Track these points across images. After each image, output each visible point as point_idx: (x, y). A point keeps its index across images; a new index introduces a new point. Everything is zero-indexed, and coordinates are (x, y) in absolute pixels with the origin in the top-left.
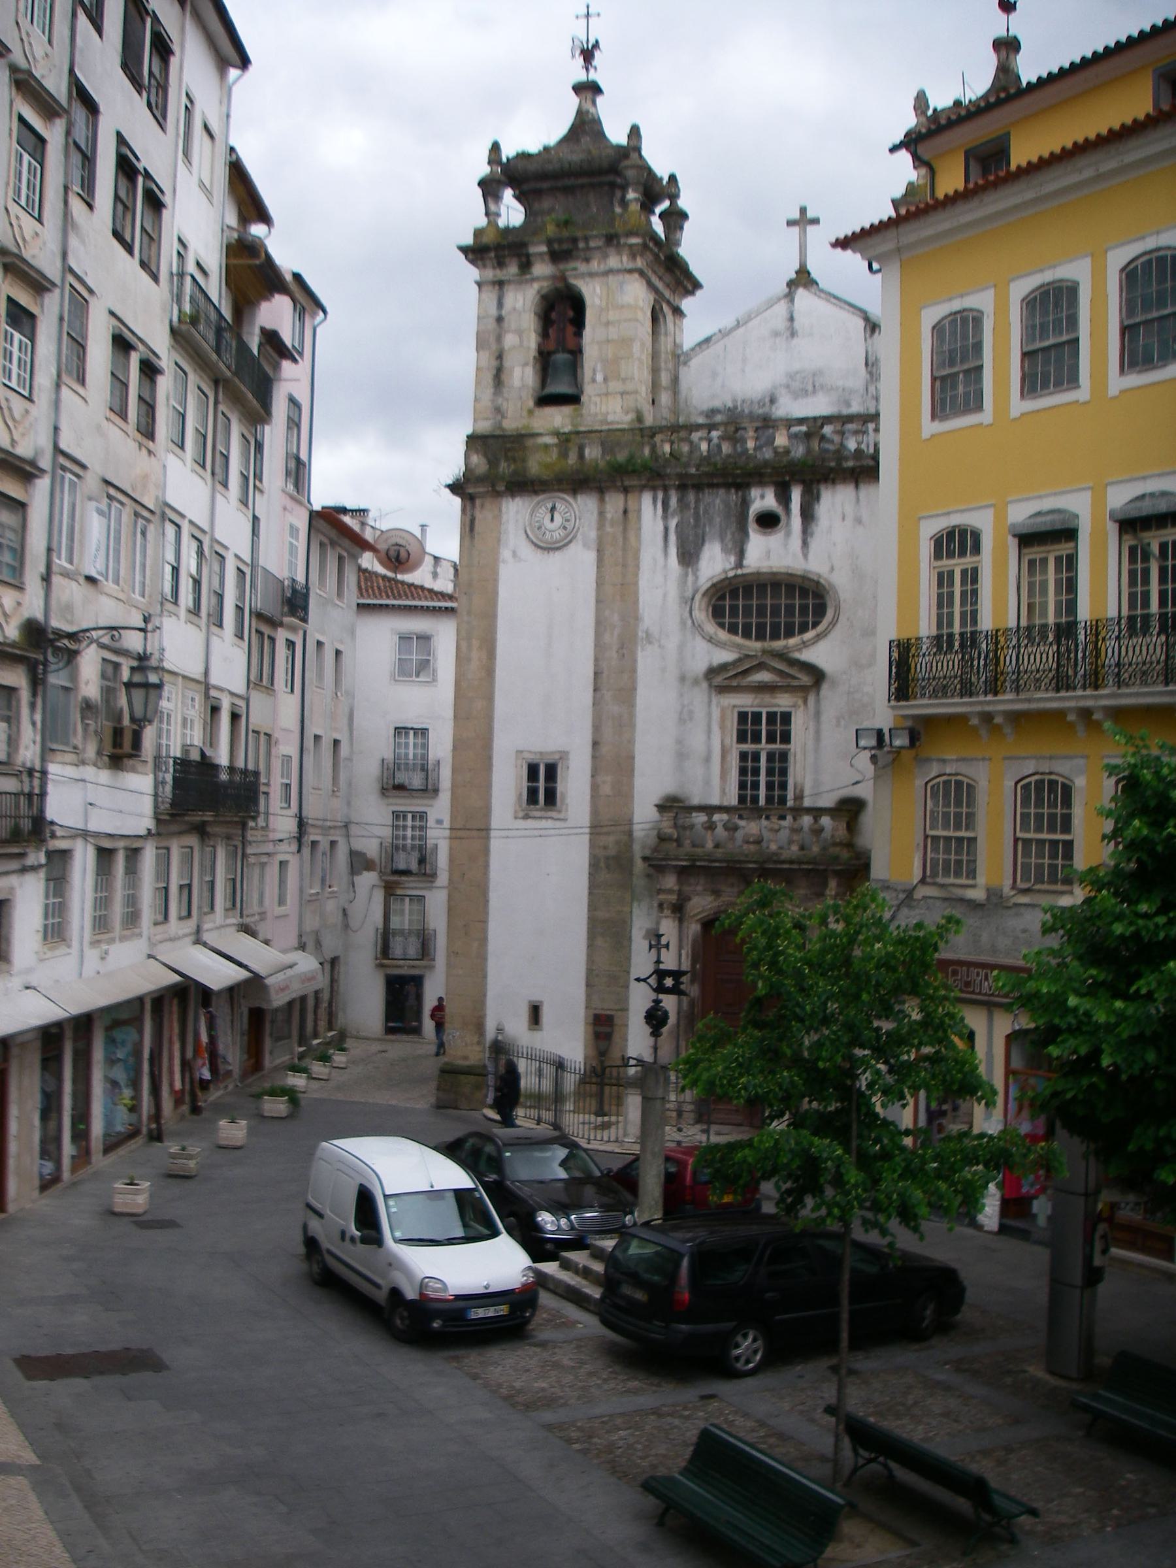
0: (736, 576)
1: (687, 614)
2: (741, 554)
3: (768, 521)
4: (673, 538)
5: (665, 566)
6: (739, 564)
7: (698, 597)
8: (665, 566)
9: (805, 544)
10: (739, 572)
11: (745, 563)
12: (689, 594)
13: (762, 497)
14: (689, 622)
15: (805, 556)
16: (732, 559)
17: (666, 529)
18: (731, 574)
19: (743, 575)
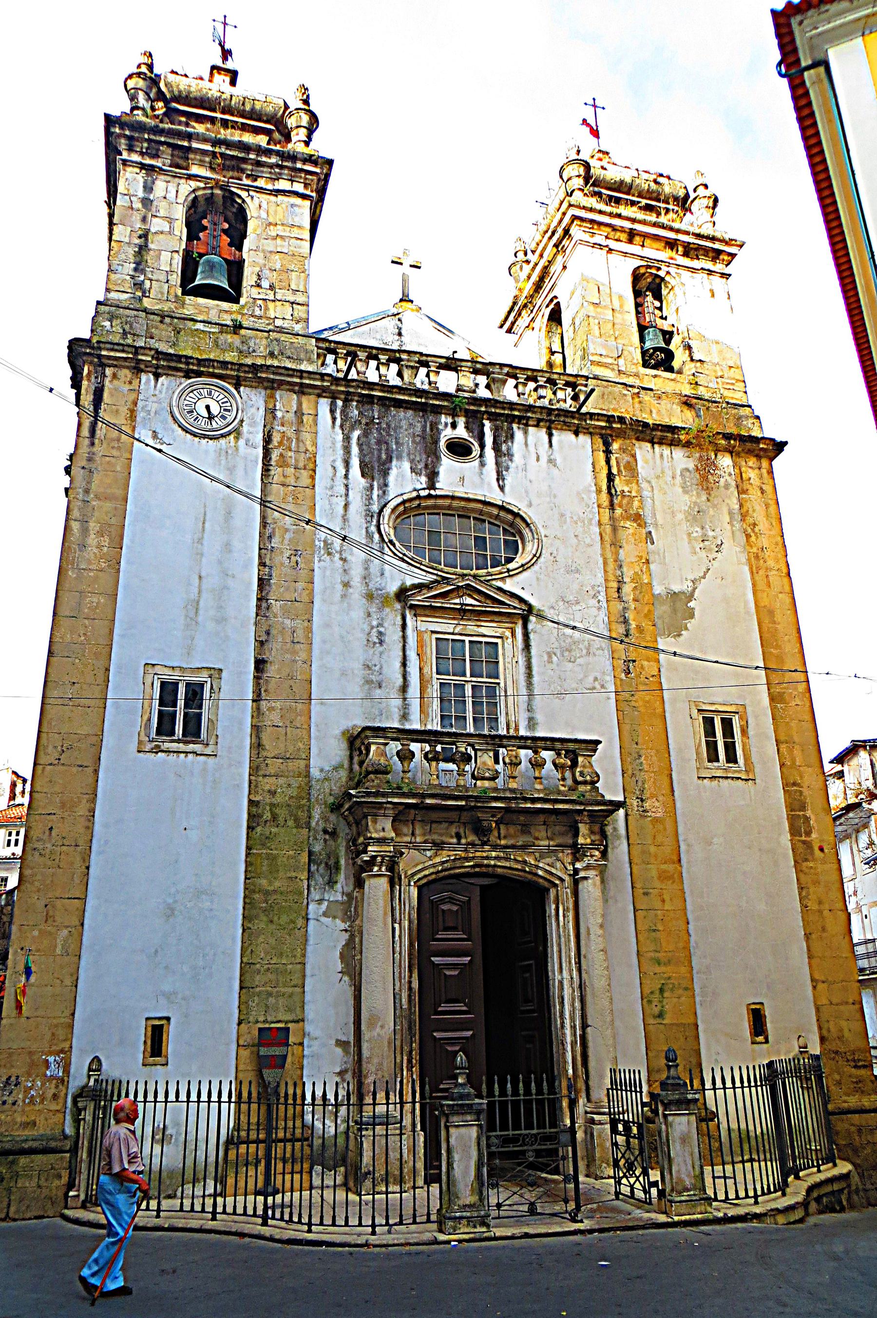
0: (430, 496)
1: (373, 529)
2: (433, 477)
3: (459, 449)
4: (355, 450)
5: (346, 476)
6: (432, 486)
7: (387, 511)
8: (346, 476)
9: (500, 477)
10: (433, 492)
11: (438, 485)
12: (375, 508)
13: (454, 426)
14: (376, 536)
15: (502, 488)
16: (424, 479)
17: (347, 439)
18: (423, 493)
19: (437, 497)
